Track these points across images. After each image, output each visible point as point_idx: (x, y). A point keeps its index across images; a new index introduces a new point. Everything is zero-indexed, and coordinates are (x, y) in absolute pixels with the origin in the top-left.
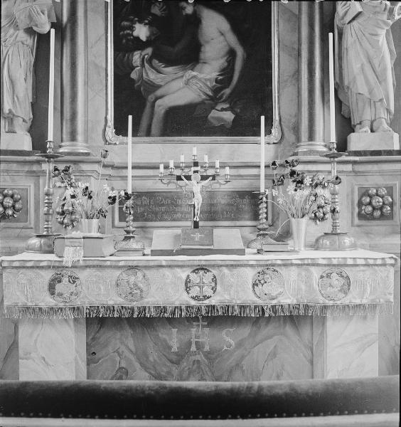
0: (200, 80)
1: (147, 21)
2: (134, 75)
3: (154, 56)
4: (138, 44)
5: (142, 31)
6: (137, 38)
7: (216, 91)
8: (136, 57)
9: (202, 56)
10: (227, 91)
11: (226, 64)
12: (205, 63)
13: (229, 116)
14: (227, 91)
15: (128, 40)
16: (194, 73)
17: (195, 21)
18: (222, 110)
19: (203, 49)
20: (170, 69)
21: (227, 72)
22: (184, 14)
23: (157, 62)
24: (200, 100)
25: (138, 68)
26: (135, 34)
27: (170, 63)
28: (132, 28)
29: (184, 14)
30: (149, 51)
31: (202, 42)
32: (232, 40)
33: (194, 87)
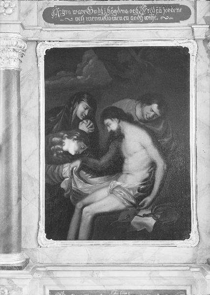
0: (124, 189)
1: (75, 137)
2: (63, 185)
3: (83, 167)
4: (68, 158)
5: (71, 146)
6: (67, 153)
7: (139, 199)
8: (66, 169)
9: (125, 167)
10: (149, 199)
11: (148, 175)
12: (128, 174)
13: (151, 221)
14: (149, 199)
15: (58, 154)
16: (118, 183)
17: (119, 136)
18: (145, 216)
19: (126, 161)
20: (96, 180)
21: (148, 183)
22: (109, 130)
23: (85, 173)
24: (122, 207)
25: (68, 179)
26: (65, 148)
27: (97, 173)
28: (61, 143)
29: (109, 130)
30: (77, 163)
31: (125, 154)
32: (155, 154)
33: (118, 195)
